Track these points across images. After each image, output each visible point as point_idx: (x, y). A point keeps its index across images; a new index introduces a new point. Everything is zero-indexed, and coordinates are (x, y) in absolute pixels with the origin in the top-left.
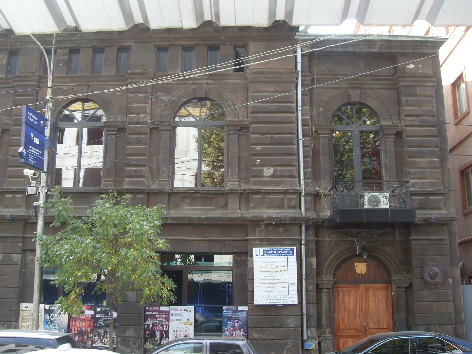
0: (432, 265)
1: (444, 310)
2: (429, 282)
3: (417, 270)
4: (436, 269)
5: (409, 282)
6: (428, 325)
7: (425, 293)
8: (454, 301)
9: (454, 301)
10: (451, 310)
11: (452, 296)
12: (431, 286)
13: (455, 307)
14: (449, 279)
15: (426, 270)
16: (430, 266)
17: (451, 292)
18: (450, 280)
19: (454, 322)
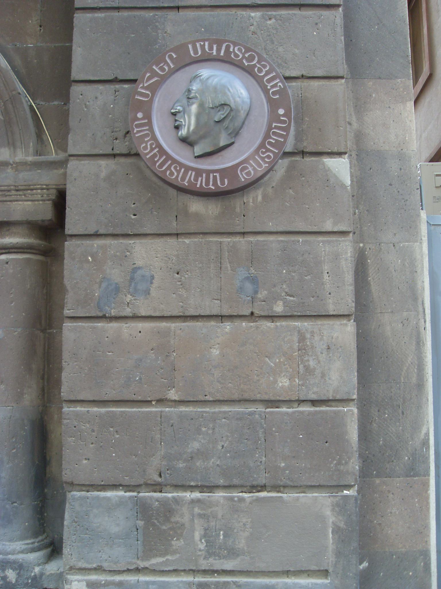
0: (206, 59)
1: (284, 382)
2: (175, 175)
3: (91, 103)
4: (238, 90)
5: (48, 178)
6: (158, 487)
7: (145, 254)
8: (362, 311)
9: (362, 311)
10: (339, 375)
11: (349, 278)
12: (196, 206)
13: (368, 354)
14: (330, 162)
15: (154, 89)
16: (185, 62)
17: (346, 248)
18: (341, 168)
19: (354, 465)
